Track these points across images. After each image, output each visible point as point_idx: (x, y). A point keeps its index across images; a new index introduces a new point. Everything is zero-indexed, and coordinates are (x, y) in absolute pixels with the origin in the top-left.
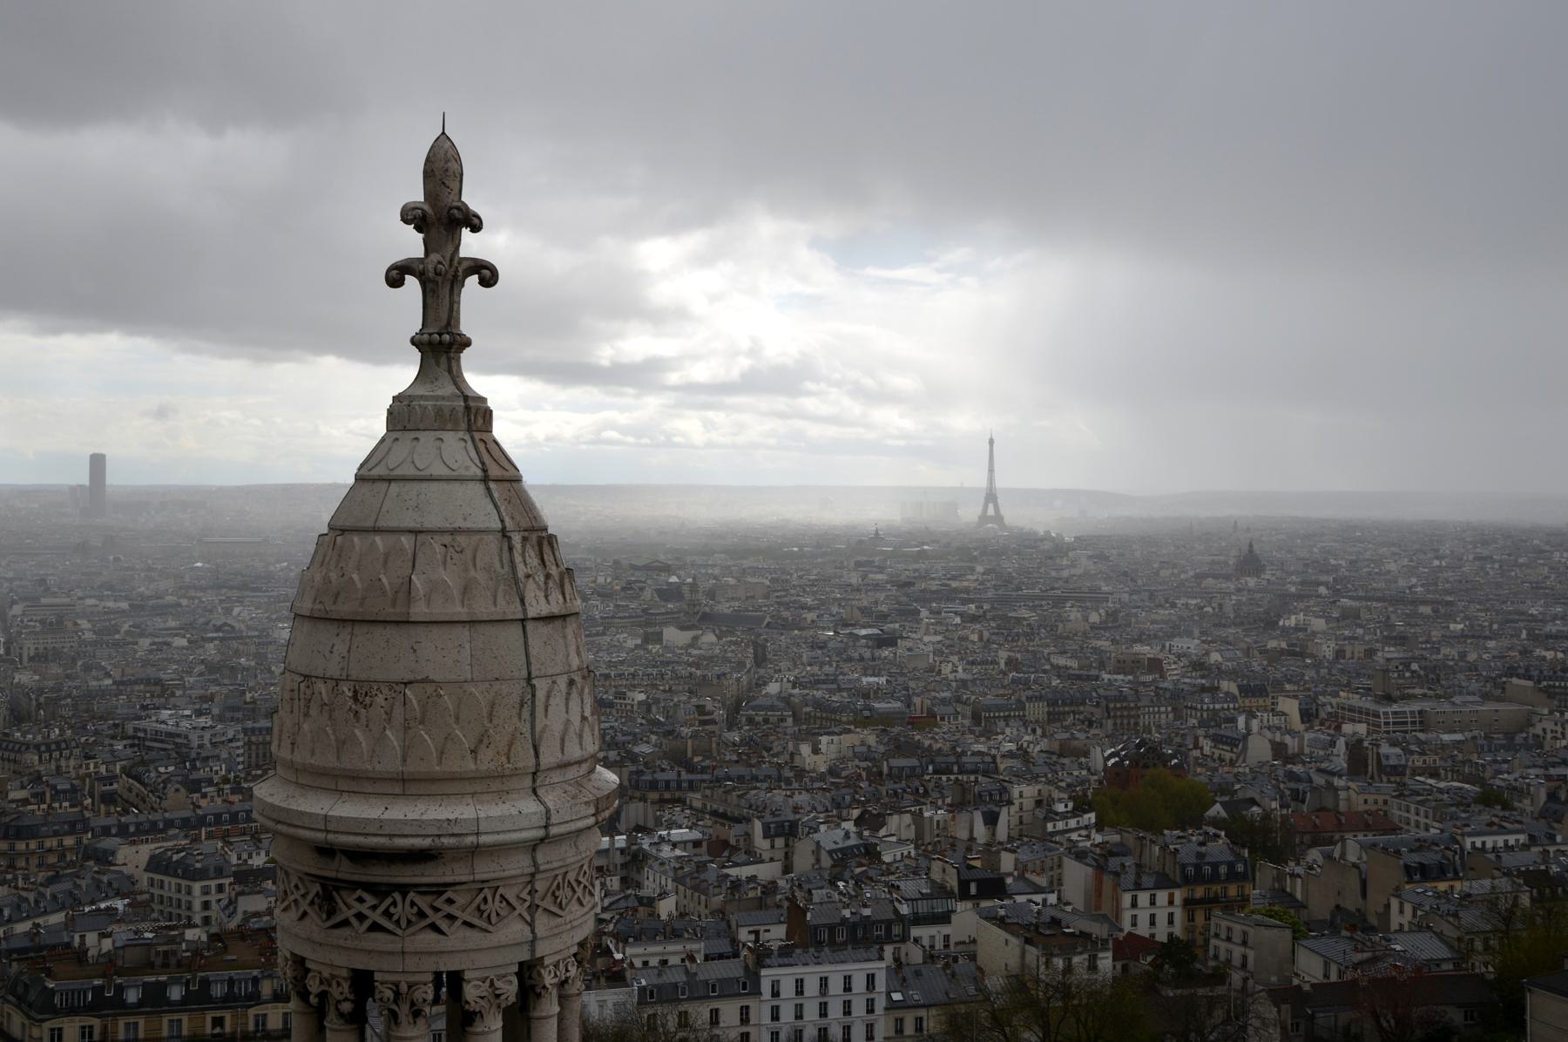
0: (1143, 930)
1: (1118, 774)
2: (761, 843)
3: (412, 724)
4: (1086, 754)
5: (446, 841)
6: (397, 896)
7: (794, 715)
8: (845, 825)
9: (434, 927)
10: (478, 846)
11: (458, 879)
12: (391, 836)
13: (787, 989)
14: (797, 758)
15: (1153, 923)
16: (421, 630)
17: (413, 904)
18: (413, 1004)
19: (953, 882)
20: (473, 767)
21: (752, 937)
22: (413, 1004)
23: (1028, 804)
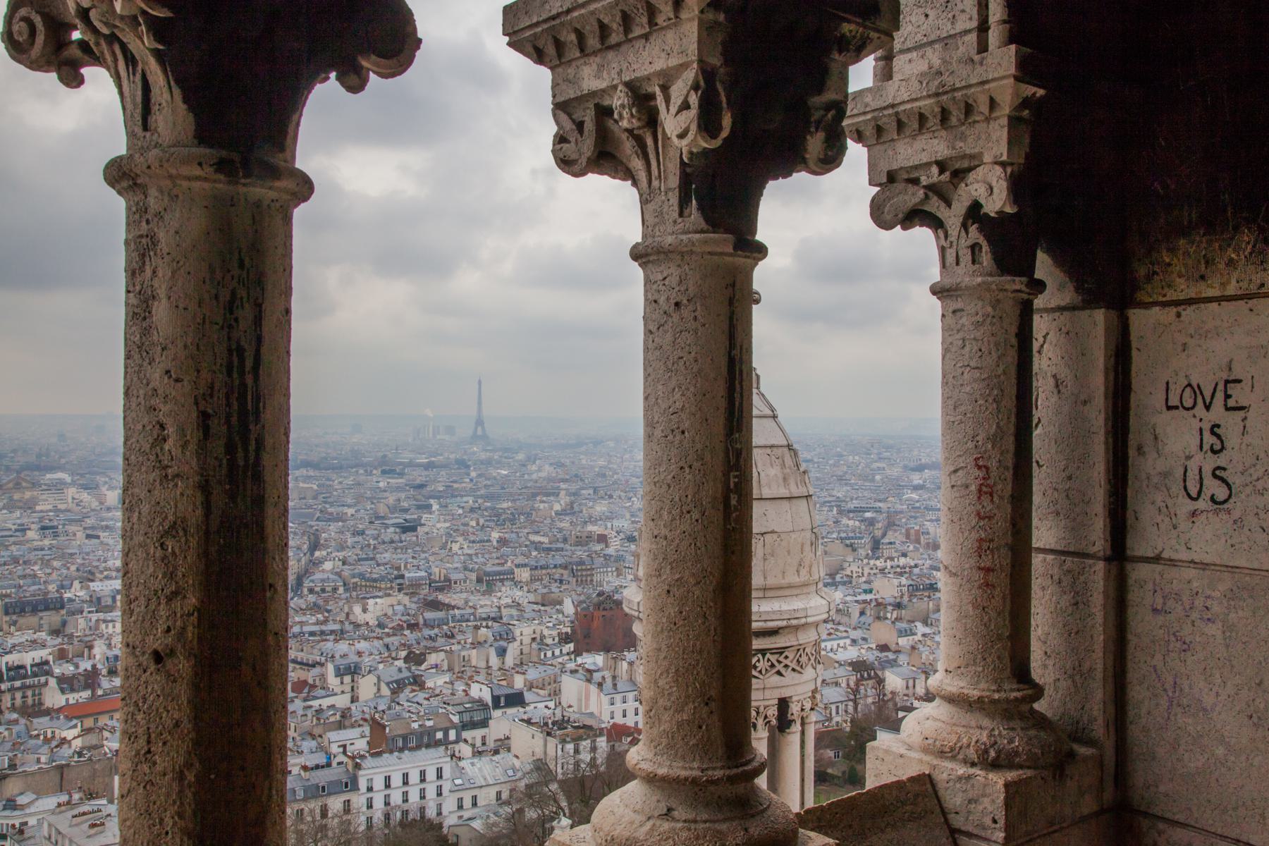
0: (619, 720)
1: (585, 616)
2: (333, 681)
3: (768, 557)
4: (561, 603)
5: (794, 622)
6: (760, 656)
7: (345, 585)
8: (397, 663)
9: (779, 673)
10: (806, 624)
11: (788, 645)
12: (765, 621)
13: (379, 784)
14: (351, 617)
15: (624, 716)
16: (768, 502)
17: (769, 660)
18: (766, 717)
19: (488, 698)
20: (798, 580)
21: (341, 750)
22: (766, 717)
23: (527, 640)
